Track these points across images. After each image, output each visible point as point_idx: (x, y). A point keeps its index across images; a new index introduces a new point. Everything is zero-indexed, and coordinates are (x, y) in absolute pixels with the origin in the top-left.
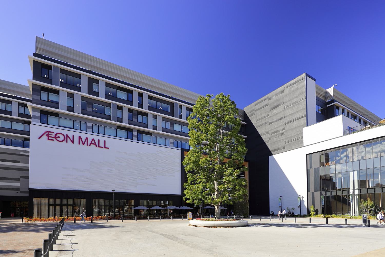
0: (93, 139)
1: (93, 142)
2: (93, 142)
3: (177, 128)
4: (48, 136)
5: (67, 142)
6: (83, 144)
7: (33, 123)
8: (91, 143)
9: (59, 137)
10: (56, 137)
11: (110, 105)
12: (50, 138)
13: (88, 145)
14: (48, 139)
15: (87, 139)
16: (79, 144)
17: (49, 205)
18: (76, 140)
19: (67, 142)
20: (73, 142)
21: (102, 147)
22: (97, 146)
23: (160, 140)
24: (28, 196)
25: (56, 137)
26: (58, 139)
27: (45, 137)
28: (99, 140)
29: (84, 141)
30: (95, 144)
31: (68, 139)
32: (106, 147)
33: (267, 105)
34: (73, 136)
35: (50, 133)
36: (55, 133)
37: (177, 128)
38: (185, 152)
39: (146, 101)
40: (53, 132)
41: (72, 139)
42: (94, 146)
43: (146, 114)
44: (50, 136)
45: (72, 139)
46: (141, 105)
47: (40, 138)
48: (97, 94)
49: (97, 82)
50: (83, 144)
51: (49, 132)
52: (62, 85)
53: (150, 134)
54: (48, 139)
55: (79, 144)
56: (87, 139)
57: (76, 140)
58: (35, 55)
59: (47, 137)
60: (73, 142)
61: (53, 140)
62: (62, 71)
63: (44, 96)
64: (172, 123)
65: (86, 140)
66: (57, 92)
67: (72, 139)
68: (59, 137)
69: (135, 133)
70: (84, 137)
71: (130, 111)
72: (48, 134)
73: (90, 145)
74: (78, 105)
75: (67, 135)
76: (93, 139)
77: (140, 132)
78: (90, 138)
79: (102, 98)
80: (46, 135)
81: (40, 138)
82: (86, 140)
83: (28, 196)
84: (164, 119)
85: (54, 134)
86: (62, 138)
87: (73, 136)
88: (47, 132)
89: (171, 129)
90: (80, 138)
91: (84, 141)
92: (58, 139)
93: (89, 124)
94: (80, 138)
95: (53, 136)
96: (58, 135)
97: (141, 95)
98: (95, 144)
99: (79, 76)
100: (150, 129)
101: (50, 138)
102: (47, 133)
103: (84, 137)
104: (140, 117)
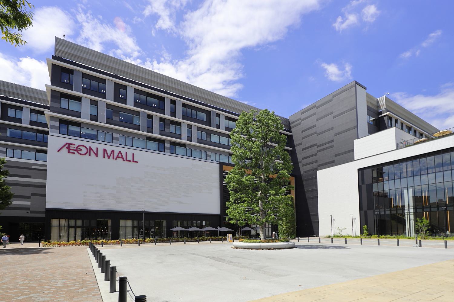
0: (120, 152)
1: (120, 155)
2: (120, 155)
3: (214, 138)
4: (68, 148)
5: (90, 155)
6: (109, 157)
7: (51, 133)
8: (118, 157)
9: (81, 150)
10: (78, 149)
11: (138, 113)
12: (71, 151)
13: (113, 159)
14: (69, 152)
15: (113, 151)
16: (104, 157)
17: (69, 227)
18: (100, 153)
19: (90, 155)
20: (96, 155)
21: (130, 161)
22: (124, 160)
23: (196, 153)
24: (45, 216)
25: (78, 150)
26: (80, 152)
27: (65, 150)
28: (126, 153)
29: (109, 154)
30: (122, 157)
31: (92, 152)
32: (135, 160)
33: (314, 114)
34: (97, 148)
35: (71, 146)
36: (77, 145)
37: (214, 138)
38: (224, 166)
39: (179, 109)
40: (74, 145)
41: (95, 152)
42: (121, 159)
43: (179, 124)
44: (71, 148)
45: (95, 151)
46: (174, 114)
47: (59, 151)
48: (124, 101)
49: (125, 87)
50: (109, 157)
51: (69, 144)
52: (84, 91)
53: (183, 145)
55: (104, 157)
56: (113, 151)
57: (100, 153)
58: (54, 57)
59: (67, 150)
60: (96, 155)
61: (74, 153)
62: (85, 75)
63: (64, 103)
64: (209, 133)
65: (112, 153)
66: (79, 99)
67: (95, 152)
68: (81, 150)
69: (167, 145)
70: (109, 149)
71: (162, 120)
72: (68, 146)
73: (116, 159)
74: (102, 113)
75: (90, 147)
76: (120, 152)
77: (173, 144)
78: (117, 150)
79: (130, 106)
80: (67, 148)
81: (59, 151)
82: (112, 153)
83: (45, 216)
84: (199, 129)
85: (76, 146)
86: (84, 151)
87: (97, 148)
88: (67, 143)
89: (208, 140)
90: (105, 150)
91: (109, 154)
92: (80, 152)
93: (116, 135)
94: (105, 150)
96: (80, 147)
97: (173, 102)
98: (122, 157)
99: (104, 81)
100: (184, 141)
101: (71, 151)
102: (67, 146)
103: (109, 149)
104: (172, 128)
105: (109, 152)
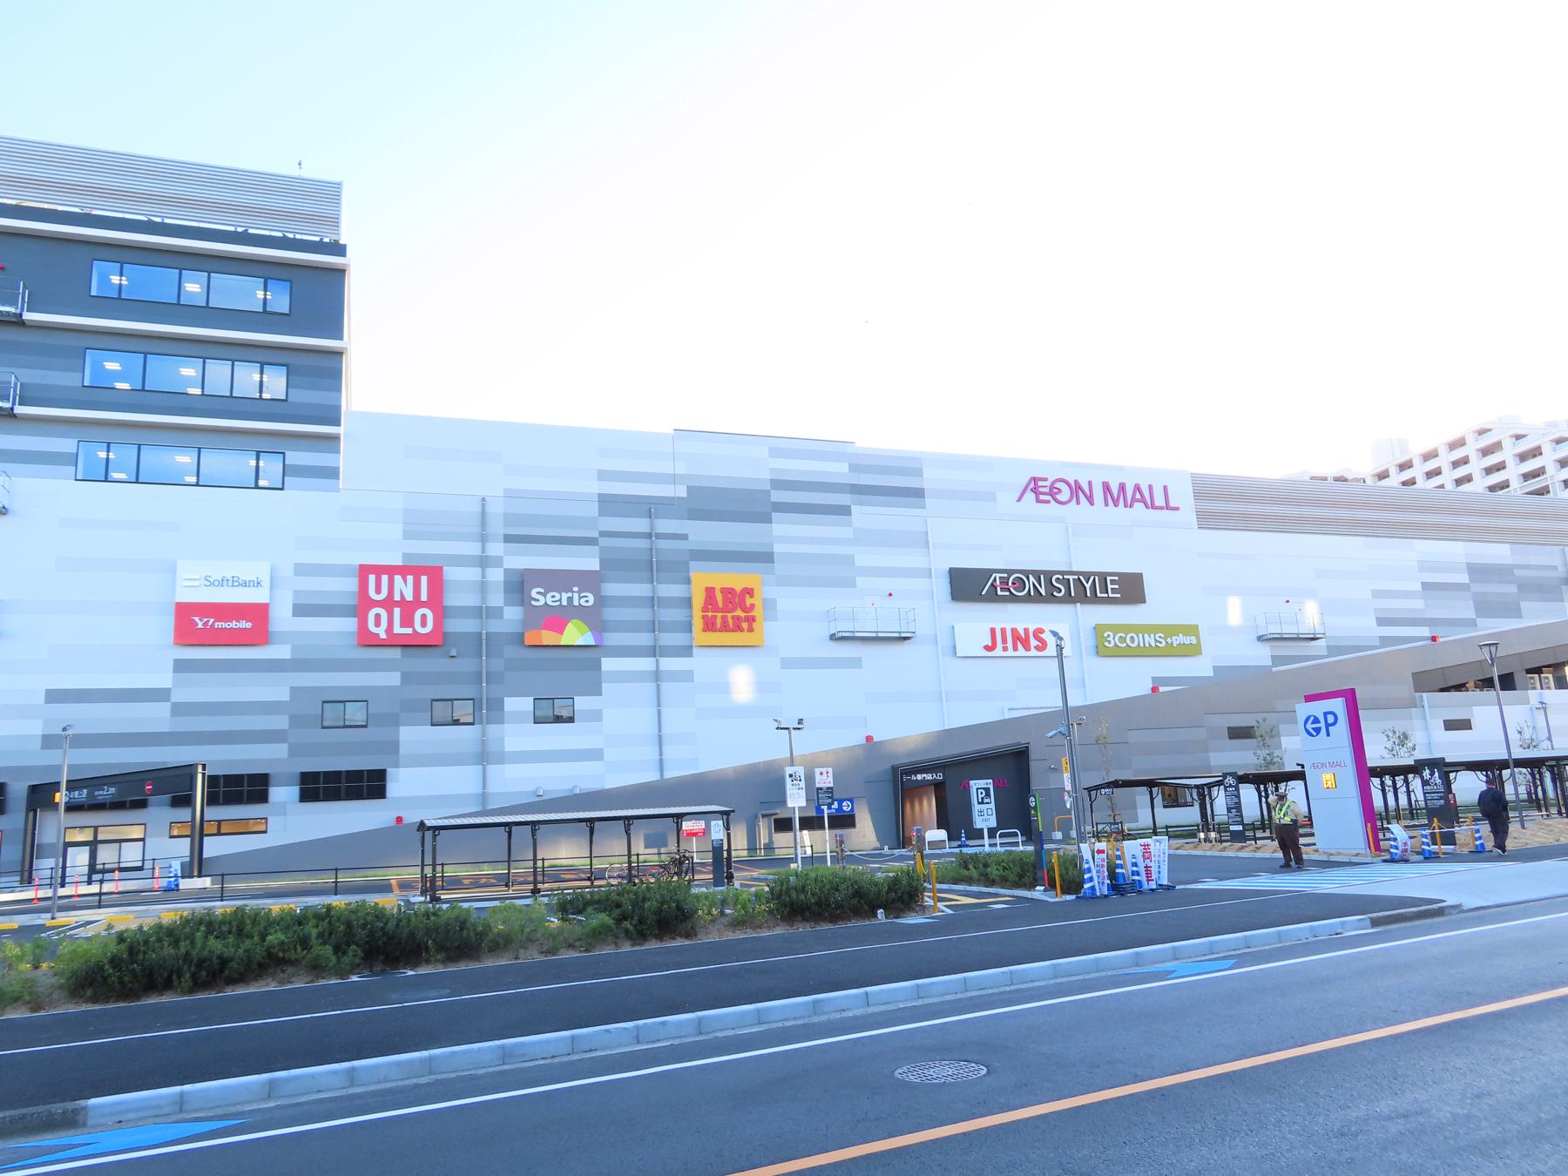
2: (1138, 496)
4: (1035, 490)
5: (1078, 503)
6: (1116, 505)
8: (1134, 500)
10: (1055, 490)
12: (1042, 497)
13: (1126, 506)
14: (1038, 501)
19: (1078, 503)
20: (1090, 499)
22: (1147, 507)
26: (1059, 497)
27: (1030, 496)
30: (1143, 500)
31: (1081, 495)
35: (1040, 483)
36: (1051, 479)
40: (1045, 479)
44: (1040, 489)
47: (1019, 500)
50: (1116, 505)
51: (1035, 479)
54: (1038, 501)
59: (1033, 495)
60: (1090, 499)
61: (1047, 502)
68: (1060, 491)
75: (1076, 481)
76: (1137, 488)
81: (1019, 500)
85: (1047, 484)
86: (1065, 495)
92: (1058, 497)
95: (1047, 490)
98: (1143, 500)
101: (1042, 497)
102: (1032, 485)
105: (1115, 489)
